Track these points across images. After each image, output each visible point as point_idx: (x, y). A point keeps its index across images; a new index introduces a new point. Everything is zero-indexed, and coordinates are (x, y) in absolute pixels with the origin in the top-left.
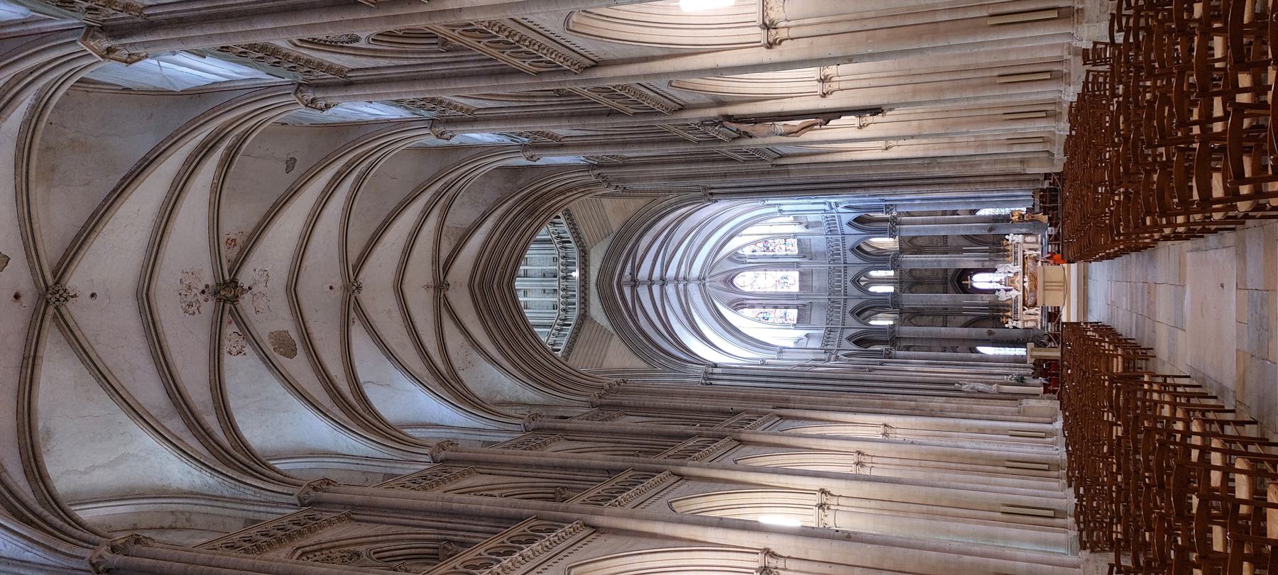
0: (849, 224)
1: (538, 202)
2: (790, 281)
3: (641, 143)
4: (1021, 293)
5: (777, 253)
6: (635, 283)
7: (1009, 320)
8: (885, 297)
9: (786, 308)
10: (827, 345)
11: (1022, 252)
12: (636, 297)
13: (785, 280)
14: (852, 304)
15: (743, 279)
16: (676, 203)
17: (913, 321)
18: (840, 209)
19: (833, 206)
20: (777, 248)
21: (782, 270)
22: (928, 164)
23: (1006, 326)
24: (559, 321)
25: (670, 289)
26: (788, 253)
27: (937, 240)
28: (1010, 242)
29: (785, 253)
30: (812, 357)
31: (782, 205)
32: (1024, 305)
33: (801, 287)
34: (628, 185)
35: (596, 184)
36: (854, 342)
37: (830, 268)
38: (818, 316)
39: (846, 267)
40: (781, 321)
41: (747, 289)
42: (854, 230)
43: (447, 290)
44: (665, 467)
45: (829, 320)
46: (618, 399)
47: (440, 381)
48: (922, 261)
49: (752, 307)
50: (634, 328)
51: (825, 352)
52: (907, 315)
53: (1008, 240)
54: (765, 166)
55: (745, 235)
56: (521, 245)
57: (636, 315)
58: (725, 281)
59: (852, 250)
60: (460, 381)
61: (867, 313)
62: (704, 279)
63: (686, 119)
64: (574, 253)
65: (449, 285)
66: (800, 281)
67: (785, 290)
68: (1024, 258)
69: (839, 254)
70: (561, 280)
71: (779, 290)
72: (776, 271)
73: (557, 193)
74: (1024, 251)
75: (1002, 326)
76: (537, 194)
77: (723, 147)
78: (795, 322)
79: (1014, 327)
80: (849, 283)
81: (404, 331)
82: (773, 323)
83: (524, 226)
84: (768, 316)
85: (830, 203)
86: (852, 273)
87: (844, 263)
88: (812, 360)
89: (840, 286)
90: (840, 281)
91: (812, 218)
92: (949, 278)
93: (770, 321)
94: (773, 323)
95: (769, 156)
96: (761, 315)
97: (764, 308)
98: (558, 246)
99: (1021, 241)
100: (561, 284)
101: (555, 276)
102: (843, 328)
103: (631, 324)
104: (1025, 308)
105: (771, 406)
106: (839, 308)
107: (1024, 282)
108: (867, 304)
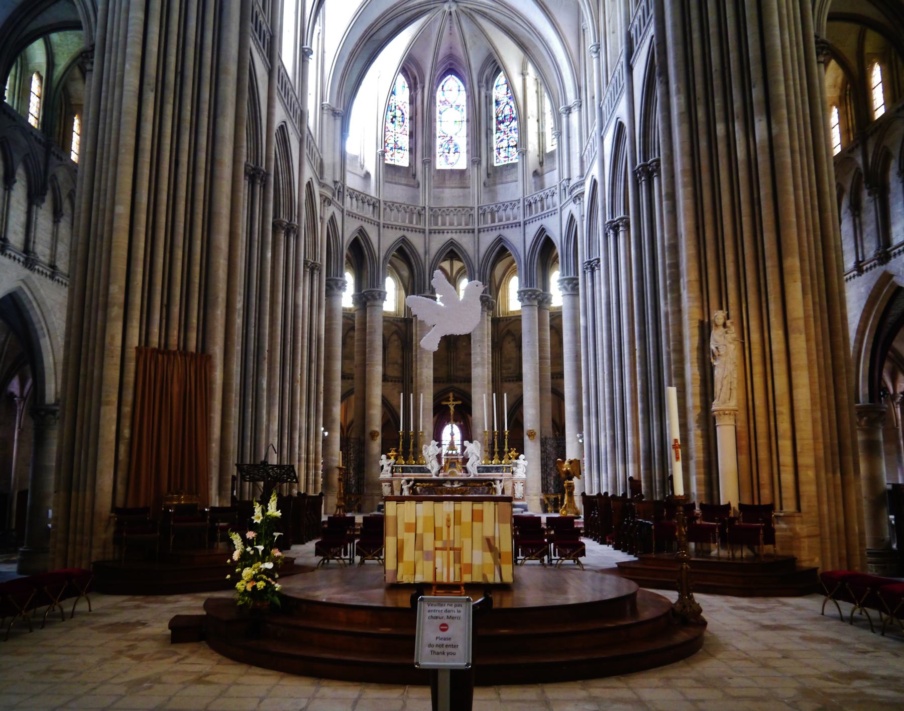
0: (542, 230)
2: (452, 157)
4: (434, 477)
5: (495, 136)
7: (392, 460)
9: (411, 150)
10: (351, 198)
11: (500, 478)
13: (452, 150)
14: (417, 240)
15: (455, 89)
17: (395, 337)
19: (576, 192)
20: (502, 135)
21: (468, 144)
23: (384, 457)
26: (495, 153)
27: (510, 368)
28: (515, 461)
29: (495, 148)
30: (328, 160)
31: (580, 111)
32: (416, 481)
33: (443, 172)
36: (356, 240)
37: (472, 208)
38: (398, 193)
39: (473, 231)
40: (391, 141)
41: (439, 95)
42: (532, 237)
45: (391, 205)
48: (483, 341)
49: (412, 101)
51: (335, 182)
52: (403, 329)
53: (517, 458)
55: (524, 80)
58: (451, 56)
59: (500, 239)
61: (405, 273)
66: (451, 170)
67: (438, 150)
69: (493, 221)
71: (439, 141)
72: (467, 136)
75: (385, 450)
78: (388, 162)
79: (382, 467)
80: (448, 237)
82: (385, 130)
84: (397, 123)
85: (582, 184)
86: (466, 242)
87: (479, 231)
88: (321, 160)
89: (444, 224)
91: (552, 179)
92: (456, 385)
93: (390, 126)
94: (385, 130)
96: (398, 113)
97: (411, 119)
99: (517, 476)
102: (378, 225)
104: (411, 483)
106: (411, 222)
107: (452, 482)
108: (418, 264)
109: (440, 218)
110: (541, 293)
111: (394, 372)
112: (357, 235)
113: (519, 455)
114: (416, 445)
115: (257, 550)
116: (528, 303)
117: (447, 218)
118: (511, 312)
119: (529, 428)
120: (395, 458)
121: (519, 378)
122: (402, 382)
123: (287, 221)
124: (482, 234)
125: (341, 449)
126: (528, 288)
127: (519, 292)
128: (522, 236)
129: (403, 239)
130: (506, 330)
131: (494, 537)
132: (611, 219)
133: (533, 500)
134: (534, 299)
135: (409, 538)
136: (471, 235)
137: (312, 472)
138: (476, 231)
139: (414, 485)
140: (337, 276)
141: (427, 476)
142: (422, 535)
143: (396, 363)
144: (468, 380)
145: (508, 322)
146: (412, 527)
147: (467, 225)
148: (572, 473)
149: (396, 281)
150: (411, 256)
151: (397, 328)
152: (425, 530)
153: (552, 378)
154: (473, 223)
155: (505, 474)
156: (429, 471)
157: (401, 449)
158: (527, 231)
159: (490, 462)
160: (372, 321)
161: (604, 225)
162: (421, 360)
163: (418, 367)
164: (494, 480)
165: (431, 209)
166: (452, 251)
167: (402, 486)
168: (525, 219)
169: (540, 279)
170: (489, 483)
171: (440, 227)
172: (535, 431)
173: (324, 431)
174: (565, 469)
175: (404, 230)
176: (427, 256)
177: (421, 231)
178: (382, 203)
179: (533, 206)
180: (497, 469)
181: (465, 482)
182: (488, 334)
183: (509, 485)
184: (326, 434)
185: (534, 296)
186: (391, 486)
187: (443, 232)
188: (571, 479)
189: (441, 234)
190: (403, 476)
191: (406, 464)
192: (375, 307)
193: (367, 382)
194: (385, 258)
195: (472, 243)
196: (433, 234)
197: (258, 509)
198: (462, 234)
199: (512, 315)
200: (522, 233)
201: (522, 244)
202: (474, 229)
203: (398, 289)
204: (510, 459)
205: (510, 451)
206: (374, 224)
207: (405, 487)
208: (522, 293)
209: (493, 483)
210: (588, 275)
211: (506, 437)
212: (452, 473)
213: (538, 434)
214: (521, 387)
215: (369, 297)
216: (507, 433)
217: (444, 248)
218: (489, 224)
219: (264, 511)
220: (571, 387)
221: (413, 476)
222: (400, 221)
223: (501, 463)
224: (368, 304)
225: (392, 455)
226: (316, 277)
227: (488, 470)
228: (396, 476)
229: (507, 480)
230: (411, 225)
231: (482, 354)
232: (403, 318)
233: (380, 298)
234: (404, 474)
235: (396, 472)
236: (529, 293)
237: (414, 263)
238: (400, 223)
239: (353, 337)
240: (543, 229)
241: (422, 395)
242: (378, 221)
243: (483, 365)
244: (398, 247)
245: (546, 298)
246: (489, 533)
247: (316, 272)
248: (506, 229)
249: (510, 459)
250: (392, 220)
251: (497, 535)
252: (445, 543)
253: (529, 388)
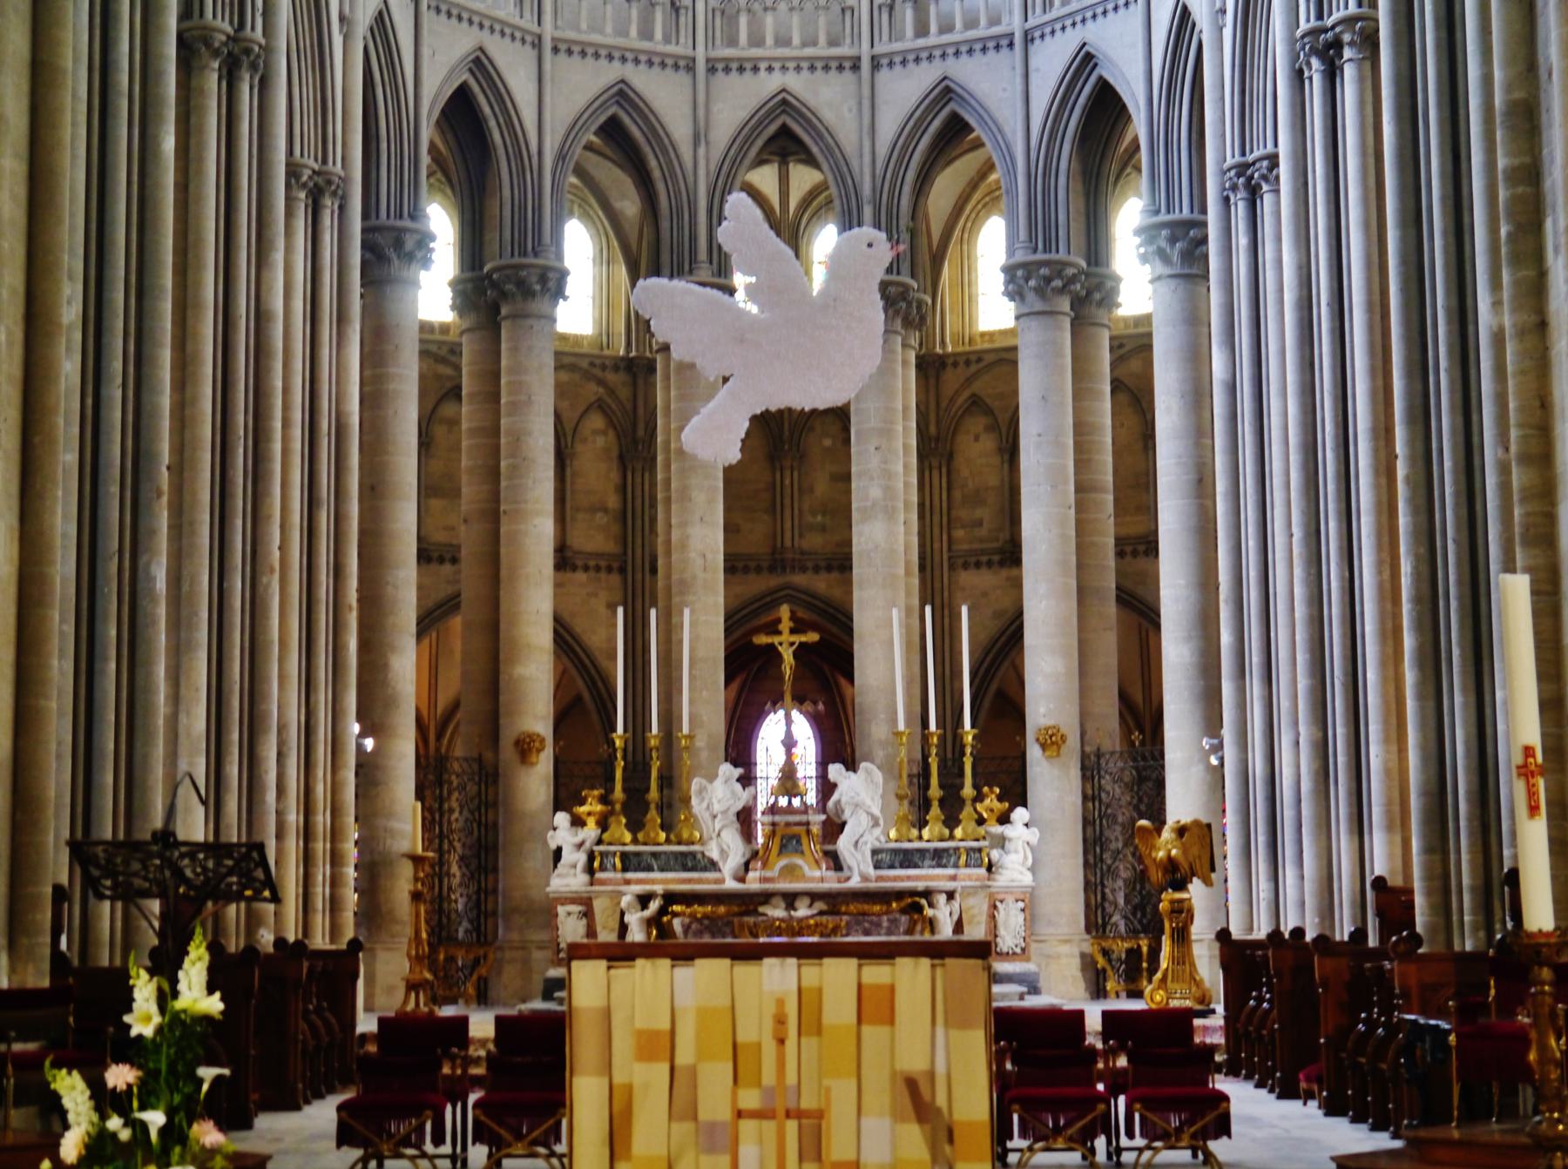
0: (1086, 60)
4: (731, 885)
7: (591, 831)
8: (702, 254)
11: (950, 885)
17: (596, 421)
23: (562, 818)
27: (980, 523)
28: (997, 829)
32: (670, 898)
39: (856, 67)
42: (1052, 83)
48: (887, 432)
52: (624, 393)
53: (1004, 819)
59: (945, 92)
61: (630, 205)
68: (914, 893)
69: (922, 30)
75: (565, 798)
79: (558, 853)
80: (769, 84)
87: (876, 64)
90: (783, 41)
92: (800, 579)
99: (1002, 880)
102: (538, 44)
104: (654, 906)
106: (646, 34)
107: (790, 899)
108: (670, 175)
109: (743, 20)
110: (1082, 272)
111: (593, 538)
112: (466, 76)
113: (1011, 809)
114: (667, 781)
115: (141, 1128)
116: (1039, 306)
117: (769, 20)
118: (983, 335)
119: (1045, 722)
120: (598, 823)
121: (1011, 554)
122: (622, 570)
123: (229, 30)
124: (884, 75)
125: (420, 794)
126: (1040, 256)
127: (1009, 271)
128: (1019, 80)
129: (621, 93)
130: (966, 394)
131: (931, 1075)
132: (1313, 23)
133: (1058, 957)
134: (1061, 291)
135: (650, 1080)
136: (848, 75)
137: (322, 872)
138: (866, 65)
139: (663, 911)
140: (401, 217)
141: (708, 881)
142: (693, 1072)
144: (841, 563)
145: (974, 368)
146: (658, 1045)
147: (833, 43)
148: (1185, 865)
149: (597, 233)
150: (647, 149)
151: (601, 390)
152: (702, 1053)
153: (1120, 554)
154: (856, 37)
155: (963, 872)
156: (713, 866)
157: (618, 793)
158: (1034, 62)
159: (915, 832)
160: (517, 369)
161: (1291, 41)
162: (685, 496)
163: (674, 521)
164: (927, 894)
166: (785, 131)
167: (622, 914)
168: (1028, 25)
169: (1078, 227)
170: (913, 903)
171: (742, 50)
172: (1064, 730)
173: (362, 735)
174: (1161, 854)
175: (624, 59)
176: (702, 151)
177: (682, 63)
180: (939, 857)
181: (834, 901)
182: (905, 409)
183: (977, 908)
184: (369, 743)
185: (1057, 283)
186: (588, 914)
187: (756, 69)
188: (1181, 885)
189: (748, 74)
190: (628, 882)
191: (635, 841)
192: (529, 322)
193: (503, 572)
194: (561, 156)
195: (853, 103)
196: (720, 75)
197: (144, 990)
198: (819, 73)
199: (987, 346)
200: (1019, 70)
201: (1020, 105)
202: (859, 58)
203: (603, 259)
204: (981, 821)
205: (979, 798)
206: (523, 41)
207: (634, 919)
208: (1020, 273)
209: (924, 902)
210: (1240, 210)
211: (968, 750)
212: (790, 871)
213: (1073, 741)
214: (1017, 584)
215: (509, 287)
216: (970, 738)
217: (760, 122)
218: (909, 42)
219: (165, 997)
220: (1182, 582)
221: (660, 881)
222: (609, 29)
223: (952, 837)
224: (504, 311)
225: (589, 814)
226: (328, 220)
227: (907, 859)
228: (603, 882)
229: (970, 892)
230: (646, 45)
231: (888, 475)
232: (622, 359)
233: (545, 289)
234: (630, 875)
235: (602, 868)
236: (1044, 271)
237: (656, 174)
238: (608, 38)
239: (454, 422)
240: (1089, 57)
241: (687, 612)
242: (534, 28)
243: (890, 513)
244: (602, 119)
245: (1099, 286)
246: (913, 1060)
247: (327, 201)
248: (964, 58)
249: (981, 821)
250: (584, 26)
251: (940, 1068)
252: (769, 1093)
253: (1043, 588)
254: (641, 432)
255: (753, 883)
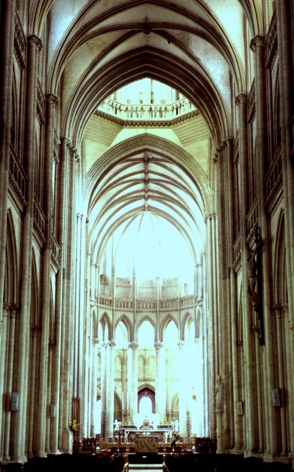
1: (207, 97)
3: (247, 180)
6: (146, 161)
12: (136, 162)
14: (130, 316)
16: (205, 193)
17: (118, 358)
18: (198, 308)
22: (228, 371)
24: (119, 105)
25: (140, 186)
34: (218, 164)
35: (219, 141)
39: (156, 312)
43: (145, 33)
44: (30, 203)
46: (67, 157)
47: (80, 31)
50: (113, 161)
52: (122, 354)
54: (230, 264)
56: (176, 84)
57: (123, 163)
60: (80, 45)
62: (148, 210)
63: (261, 217)
64: (170, 116)
65: (148, 33)
70: (149, 107)
73: (213, 112)
74: (167, 432)
76: (211, 97)
77: (242, 237)
81: (115, 5)
83: (189, 87)
85: (202, 301)
87: (159, 312)
89: (143, 307)
95: (235, 266)
98: (174, 105)
100: (146, 107)
101: (152, 102)
102: (113, 310)
103: (117, 159)
104: (128, 434)
105: (64, 267)
107: (146, 432)
122: (122, 381)
136: (155, 313)
139: (129, 434)
143: (118, 371)
158: (181, 313)
164: (164, 432)
165: (137, 301)
170: (162, 433)
178: (114, 300)
179: (184, 302)
254: (125, 360)
255: (141, 431)
